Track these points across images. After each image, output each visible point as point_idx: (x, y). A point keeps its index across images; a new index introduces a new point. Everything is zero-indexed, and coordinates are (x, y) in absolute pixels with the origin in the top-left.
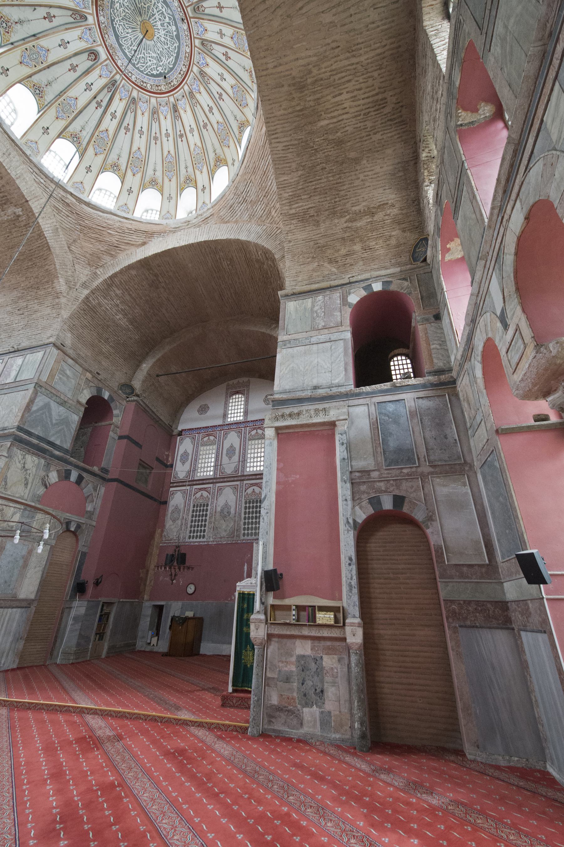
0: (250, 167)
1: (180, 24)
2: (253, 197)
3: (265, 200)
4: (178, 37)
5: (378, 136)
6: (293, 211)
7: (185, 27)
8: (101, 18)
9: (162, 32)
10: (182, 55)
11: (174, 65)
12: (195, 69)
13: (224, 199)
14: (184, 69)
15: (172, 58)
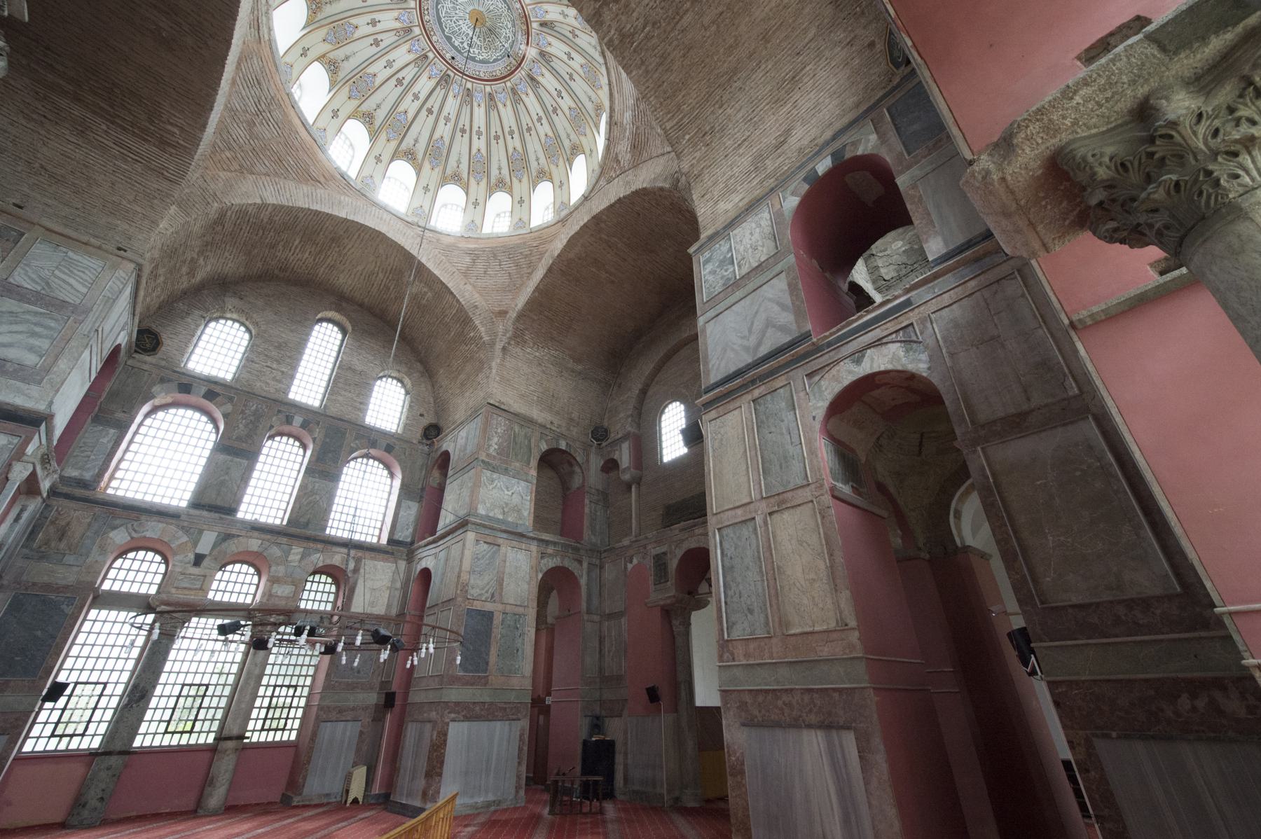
0: (296, 143)
1: (454, 53)
2: (259, 129)
3: (247, 148)
4: (449, 39)
5: (259, 265)
6: (229, 213)
7: (448, 56)
8: (518, 6)
9: (464, 28)
10: (436, 27)
11: (437, 10)
12: (417, 31)
13: (273, 69)
14: (426, 18)
15: (442, 15)
